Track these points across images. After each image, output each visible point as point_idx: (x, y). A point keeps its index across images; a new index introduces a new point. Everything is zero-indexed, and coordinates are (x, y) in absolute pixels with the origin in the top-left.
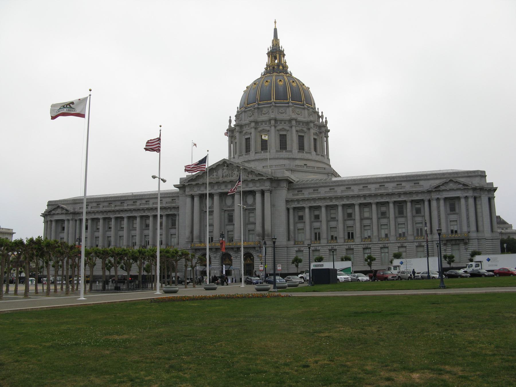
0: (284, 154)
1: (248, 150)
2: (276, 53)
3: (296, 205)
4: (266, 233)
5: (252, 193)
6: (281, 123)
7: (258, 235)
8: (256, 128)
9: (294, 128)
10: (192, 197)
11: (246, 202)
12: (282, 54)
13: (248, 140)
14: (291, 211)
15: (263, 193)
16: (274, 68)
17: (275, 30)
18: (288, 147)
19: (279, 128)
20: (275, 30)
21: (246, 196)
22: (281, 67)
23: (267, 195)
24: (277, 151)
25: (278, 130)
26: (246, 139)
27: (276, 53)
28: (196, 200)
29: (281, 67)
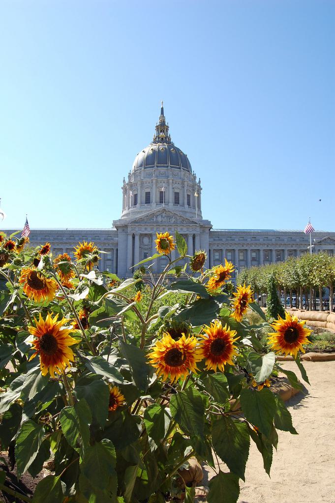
0: (178, 208)
2: (162, 127)
3: (215, 247)
5: (186, 236)
6: (176, 183)
9: (186, 188)
10: (134, 238)
13: (148, 195)
14: (212, 252)
16: (162, 139)
17: (162, 109)
20: (162, 109)
22: (167, 140)
23: (197, 239)
26: (146, 193)
27: (162, 127)
29: (167, 140)
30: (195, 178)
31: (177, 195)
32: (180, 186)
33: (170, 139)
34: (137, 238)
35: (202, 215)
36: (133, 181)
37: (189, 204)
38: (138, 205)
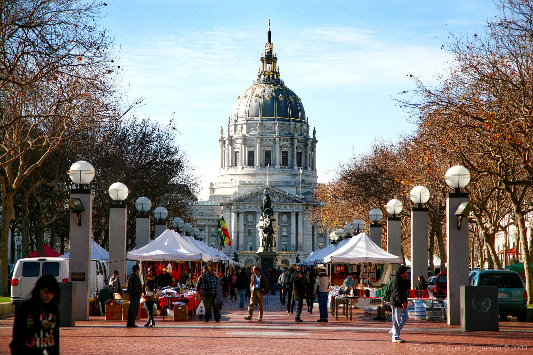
0: (287, 170)
1: (251, 163)
4: (299, 245)
5: (289, 214)
7: (293, 247)
8: (261, 144)
10: (238, 214)
11: (281, 220)
12: (276, 59)
13: (251, 155)
15: (297, 215)
17: (270, 32)
18: (289, 163)
19: (281, 144)
20: (270, 32)
21: (282, 216)
22: (275, 77)
24: (281, 168)
25: (281, 147)
27: (270, 58)
28: (242, 216)
29: (275, 77)
30: (307, 131)
31: (285, 155)
32: (288, 144)
33: (278, 74)
34: (242, 216)
35: (318, 173)
36: (232, 134)
37: (299, 165)
38: (240, 166)
